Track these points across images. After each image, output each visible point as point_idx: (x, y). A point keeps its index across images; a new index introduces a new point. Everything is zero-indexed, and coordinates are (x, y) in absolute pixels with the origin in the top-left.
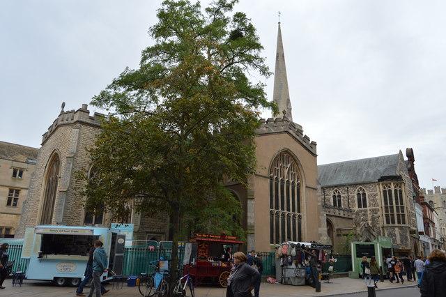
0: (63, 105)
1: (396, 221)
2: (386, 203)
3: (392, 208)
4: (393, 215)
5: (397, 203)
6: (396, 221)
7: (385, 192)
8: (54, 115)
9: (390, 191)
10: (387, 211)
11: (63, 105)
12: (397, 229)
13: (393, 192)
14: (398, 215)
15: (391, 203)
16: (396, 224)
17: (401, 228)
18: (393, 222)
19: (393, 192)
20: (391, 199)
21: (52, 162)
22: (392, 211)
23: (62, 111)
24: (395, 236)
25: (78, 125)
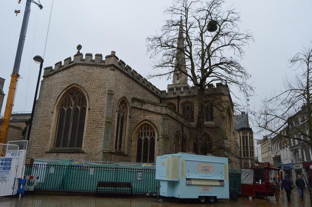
0: (79, 47)
1: (249, 155)
2: (244, 144)
3: (247, 147)
4: (247, 152)
5: (250, 145)
6: (249, 155)
7: (243, 137)
8: (72, 53)
9: (247, 137)
10: (244, 149)
11: (79, 47)
12: (249, 160)
13: (248, 138)
14: (250, 152)
15: (247, 144)
16: (250, 157)
17: (251, 159)
18: (248, 156)
19: (248, 138)
20: (247, 142)
21: (63, 95)
22: (247, 149)
23: (79, 52)
24: (248, 164)
25: (113, 68)
